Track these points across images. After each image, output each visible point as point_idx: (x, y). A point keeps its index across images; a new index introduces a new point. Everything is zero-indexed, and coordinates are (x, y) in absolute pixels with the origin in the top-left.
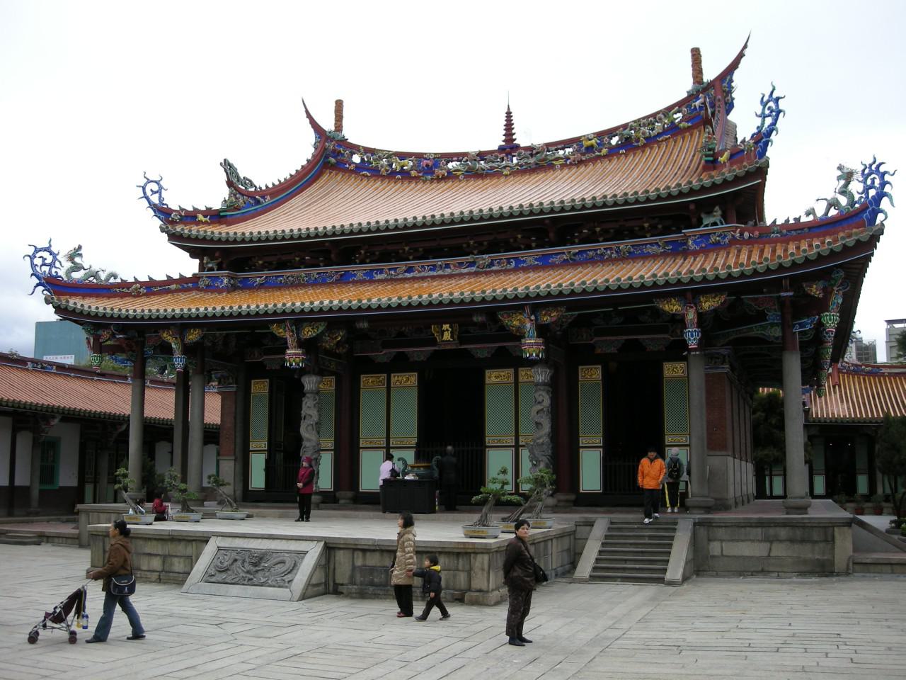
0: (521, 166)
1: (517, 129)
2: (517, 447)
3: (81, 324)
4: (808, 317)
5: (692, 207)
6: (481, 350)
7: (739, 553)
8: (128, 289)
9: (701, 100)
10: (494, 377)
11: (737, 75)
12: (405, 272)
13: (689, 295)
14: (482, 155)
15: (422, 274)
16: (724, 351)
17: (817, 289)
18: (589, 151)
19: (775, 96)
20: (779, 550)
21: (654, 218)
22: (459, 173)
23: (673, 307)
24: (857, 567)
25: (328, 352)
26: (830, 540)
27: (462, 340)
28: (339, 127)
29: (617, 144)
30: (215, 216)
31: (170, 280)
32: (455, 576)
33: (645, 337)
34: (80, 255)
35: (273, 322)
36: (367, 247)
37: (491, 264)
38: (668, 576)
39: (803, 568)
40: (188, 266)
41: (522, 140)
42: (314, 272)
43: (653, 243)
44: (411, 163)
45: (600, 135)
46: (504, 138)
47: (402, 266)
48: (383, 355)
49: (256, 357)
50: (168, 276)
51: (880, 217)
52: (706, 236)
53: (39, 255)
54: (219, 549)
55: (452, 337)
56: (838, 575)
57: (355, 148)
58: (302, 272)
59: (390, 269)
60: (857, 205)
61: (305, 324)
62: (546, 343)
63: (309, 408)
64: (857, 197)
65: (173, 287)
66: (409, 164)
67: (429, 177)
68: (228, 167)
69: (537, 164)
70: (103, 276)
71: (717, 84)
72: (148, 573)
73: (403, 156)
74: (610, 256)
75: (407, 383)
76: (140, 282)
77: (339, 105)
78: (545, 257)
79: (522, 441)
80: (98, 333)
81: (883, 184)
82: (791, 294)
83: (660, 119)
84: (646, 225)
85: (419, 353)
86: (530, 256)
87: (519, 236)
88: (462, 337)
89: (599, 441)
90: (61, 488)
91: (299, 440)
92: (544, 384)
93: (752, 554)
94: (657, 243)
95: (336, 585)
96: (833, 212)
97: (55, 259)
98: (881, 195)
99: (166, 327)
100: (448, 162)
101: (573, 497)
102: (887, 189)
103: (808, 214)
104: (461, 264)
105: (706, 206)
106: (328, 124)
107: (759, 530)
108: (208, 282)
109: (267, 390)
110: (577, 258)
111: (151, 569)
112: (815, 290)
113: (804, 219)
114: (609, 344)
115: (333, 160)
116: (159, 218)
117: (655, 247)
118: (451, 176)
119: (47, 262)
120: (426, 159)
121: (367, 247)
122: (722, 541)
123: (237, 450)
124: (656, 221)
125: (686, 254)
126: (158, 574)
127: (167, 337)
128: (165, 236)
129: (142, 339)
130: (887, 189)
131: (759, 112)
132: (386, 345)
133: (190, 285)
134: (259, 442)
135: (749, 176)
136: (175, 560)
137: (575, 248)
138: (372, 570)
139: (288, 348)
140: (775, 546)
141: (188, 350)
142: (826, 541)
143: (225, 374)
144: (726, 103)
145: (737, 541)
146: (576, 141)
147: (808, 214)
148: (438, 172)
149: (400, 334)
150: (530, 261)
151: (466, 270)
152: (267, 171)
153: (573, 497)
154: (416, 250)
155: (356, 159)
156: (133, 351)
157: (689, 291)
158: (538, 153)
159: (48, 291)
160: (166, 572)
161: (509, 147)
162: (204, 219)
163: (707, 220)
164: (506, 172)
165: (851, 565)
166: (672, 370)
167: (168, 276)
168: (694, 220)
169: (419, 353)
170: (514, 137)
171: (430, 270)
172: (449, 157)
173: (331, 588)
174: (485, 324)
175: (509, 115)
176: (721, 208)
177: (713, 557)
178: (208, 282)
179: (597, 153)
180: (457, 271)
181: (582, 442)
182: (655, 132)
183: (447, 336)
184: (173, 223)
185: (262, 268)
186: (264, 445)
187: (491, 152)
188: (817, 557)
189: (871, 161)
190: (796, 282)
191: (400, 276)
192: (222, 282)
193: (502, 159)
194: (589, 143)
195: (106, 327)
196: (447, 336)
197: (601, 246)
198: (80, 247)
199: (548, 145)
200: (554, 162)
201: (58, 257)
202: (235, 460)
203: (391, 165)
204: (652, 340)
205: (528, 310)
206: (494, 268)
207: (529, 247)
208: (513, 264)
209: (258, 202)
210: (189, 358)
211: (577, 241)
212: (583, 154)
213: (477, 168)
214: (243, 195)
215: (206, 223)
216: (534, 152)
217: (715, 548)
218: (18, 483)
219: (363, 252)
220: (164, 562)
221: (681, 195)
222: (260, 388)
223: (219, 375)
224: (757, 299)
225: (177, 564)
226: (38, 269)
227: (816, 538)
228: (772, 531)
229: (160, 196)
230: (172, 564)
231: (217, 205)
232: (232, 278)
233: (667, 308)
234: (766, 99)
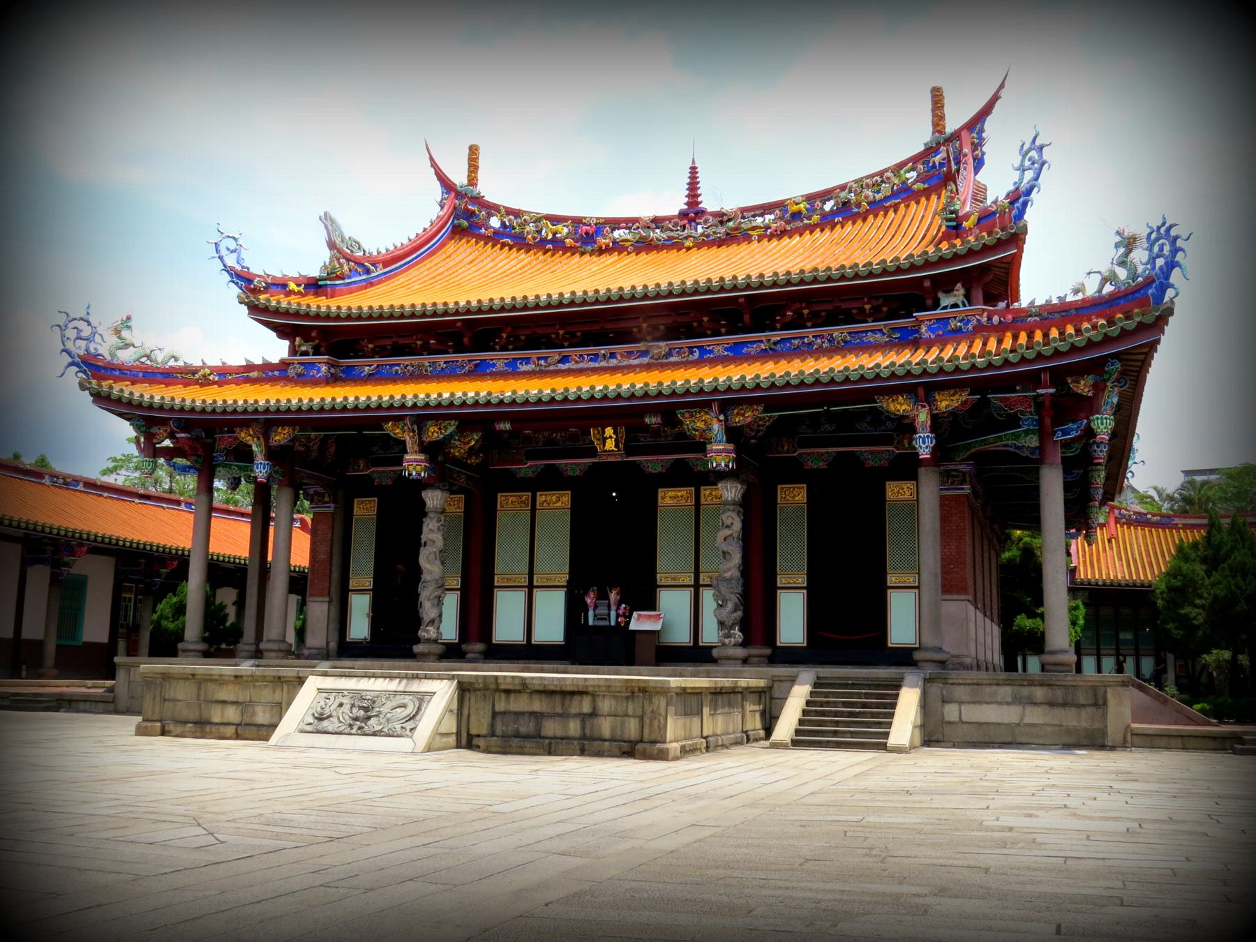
0: (708, 236)
1: (702, 190)
2: (697, 587)
3: (128, 420)
4: (1074, 421)
5: (927, 284)
6: (654, 463)
7: (983, 720)
8: (194, 373)
9: (943, 155)
10: (669, 498)
11: (990, 124)
12: (559, 362)
13: (921, 391)
14: (657, 222)
15: (581, 365)
16: (964, 468)
17: (1085, 386)
18: (792, 219)
19: (1038, 143)
20: (1034, 716)
21: (877, 298)
22: (627, 244)
23: (900, 406)
24: (1136, 739)
25: (455, 461)
26: (1099, 703)
27: (629, 450)
28: (472, 181)
29: (831, 210)
30: (314, 286)
31: (250, 367)
32: (623, 723)
33: (863, 449)
34: (129, 327)
35: (387, 419)
36: (509, 329)
37: (669, 354)
38: (892, 740)
39: (1066, 740)
40: (276, 349)
41: (709, 203)
42: (441, 359)
43: (876, 330)
44: (566, 230)
45: (810, 198)
46: (686, 200)
47: (555, 354)
48: (528, 468)
49: (362, 469)
50: (247, 361)
51: (1170, 293)
52: (944, 321)
53: (72, 325)
54: (320, 690)
55: (617, 446)
56: (1113, 748)
57: (492, 209)
58: (425, 360)
59: (539, 359)
60: (1140, 279)
61: (430, 423)
62: (737, 451)
63: (432, 533)
64: (1140, 269)
65: (254, 374)
66: (564, 230)
67: (589, 248)
68: (327, 220)
69: (728, 234)
70: (160, 357)
71: (964, 134)
73: (556, 220)
74: (821, 346)
75: (557, 504)
76: (209, 367)
77: (473, 152)
78: (736, 347)
79: (704, 579)
81: (1175, 251)
82: (1052, 391)
83: (888, 178)
84: (867, 307)
85: (573, 466)
86: (719, 344)
87: (705, 319)
88: (630, 446)
89: (802, 580)
90: (86, 644)
91: (418, 571)
92: (734, 503)
93: (999, 720)
94: (881, 330)
95: (470, 737)
96: (1108, 288)
97: (93, 334)
98: (1171, 265)
99: (245, 424)
100: (613, 230)
101: (768, 651)
102: (1179, 257)
103: (1076, 292)
104: (630, 354)
105: (945, 283)
106: (459, 177)
107: (1008, 689)
108: (300, 369)
109: (373, 512)
110: (778, 347)
112: (1083, 387)
113: (1070, 298)
114: (818, 457)
115: (465, 223)
116: (237, 284)
117: (878, 335)
118: (617, 247)
119: (84, 334)
120: (585, 224)
121: (509, 329)
122: (961, 703)
123: (333, 590)
124: (880, 301)
125: (916, 344)
127: (245, 436)
128: (244, 309)
129: (209, 441)
130: (1179, 257)
131: (1017, 165)
132: (533, 455)
133: (276, 373)
134: (363, 576)
135: (1000, 244)
137: (776, 336)
138: (518, 714)
140: (1029, 709)
141: (273, 454)
142: (1096, 705)
143: (320, 489)
144: (974, 159)
145: (980, 703)
146: (780, 205)
147: (1076, 292)
148: (602, 241)
149: (550, 442)
150: (719, 351)
152: (379, 234)
153: (768, 651)
154: (573, 335)
155: (495, 222)
156: (199, 456)
157: (922, 387)
158: (729, 220)
159: (84, 372)
160: (246, 725)
161: (693, 212)
162: (296, 289)
163: (946, 300)
164: (688, 243)
165: (1129, 736)
166: (897, 491)
167: (247, 361)
168: (929, 302)
169: (573, 466)
170: (700, 199)
171: (591, 360)
172: (615, 223)
173: (464, 741)
174: (657, 426)
175: (693, 171)
176: (963, 286)
177: (949, 723)
178: (300, 369)
179: (806, 221)
180: (625, 363)
181: (781, 581)
184: (256, 291)
185: (373, 354)
186: (368, 583)
187: (669, 219)
188: (1084, 724)
189: (1159, 224)
190: (1058, 376)
191: (552, 368)
192: (319, 371)
193: (684, 227)
194: (795, 208)
195: (163, 422)
196: (610, 445)
197: (809, 333)
198: (129, 318)
199: (743, 210)
200: (751, 233)
201: (100, 330)
202: (329, 602)
203: (539, 232)
204: (872, 453)
205: (715, 407)
206: (672, 359)
208: (697, 355)
209: (368, 271)
210: (273, 466)
211: (778, 326)
212: (788, 222)
213: (648, 238)
214: (348, 260)
215: (299, 293)
216: (725, 218)
217: (951, 712)
218: (27, 634)
219: (504, 335)
220: (242, 714)
221: (913, 268)
222: (365, 510)
223: (311, 491)
224: (1009, 398)
226: (70, 345)
227: (1082, 700)
228: (1025, 691)
229: (239, 256)
230: (254, 714)
231: (314, 272)
232: (333, 366)
233: (892, 407)
234: (1026, 148)
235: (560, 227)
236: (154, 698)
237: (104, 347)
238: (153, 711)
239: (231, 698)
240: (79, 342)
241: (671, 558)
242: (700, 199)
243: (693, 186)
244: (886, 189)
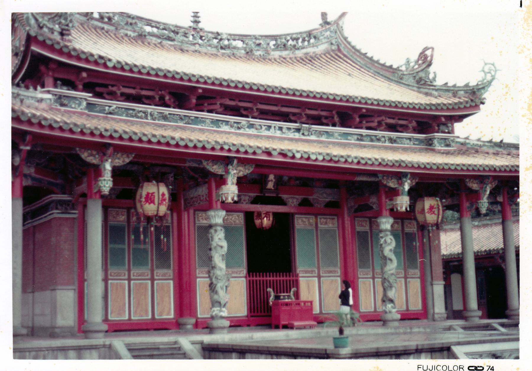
94: (410, 139)
137: (364, 132)
172: (149, 22)
207: (334, 125)
211: (364, 126)
242: (200, 19)
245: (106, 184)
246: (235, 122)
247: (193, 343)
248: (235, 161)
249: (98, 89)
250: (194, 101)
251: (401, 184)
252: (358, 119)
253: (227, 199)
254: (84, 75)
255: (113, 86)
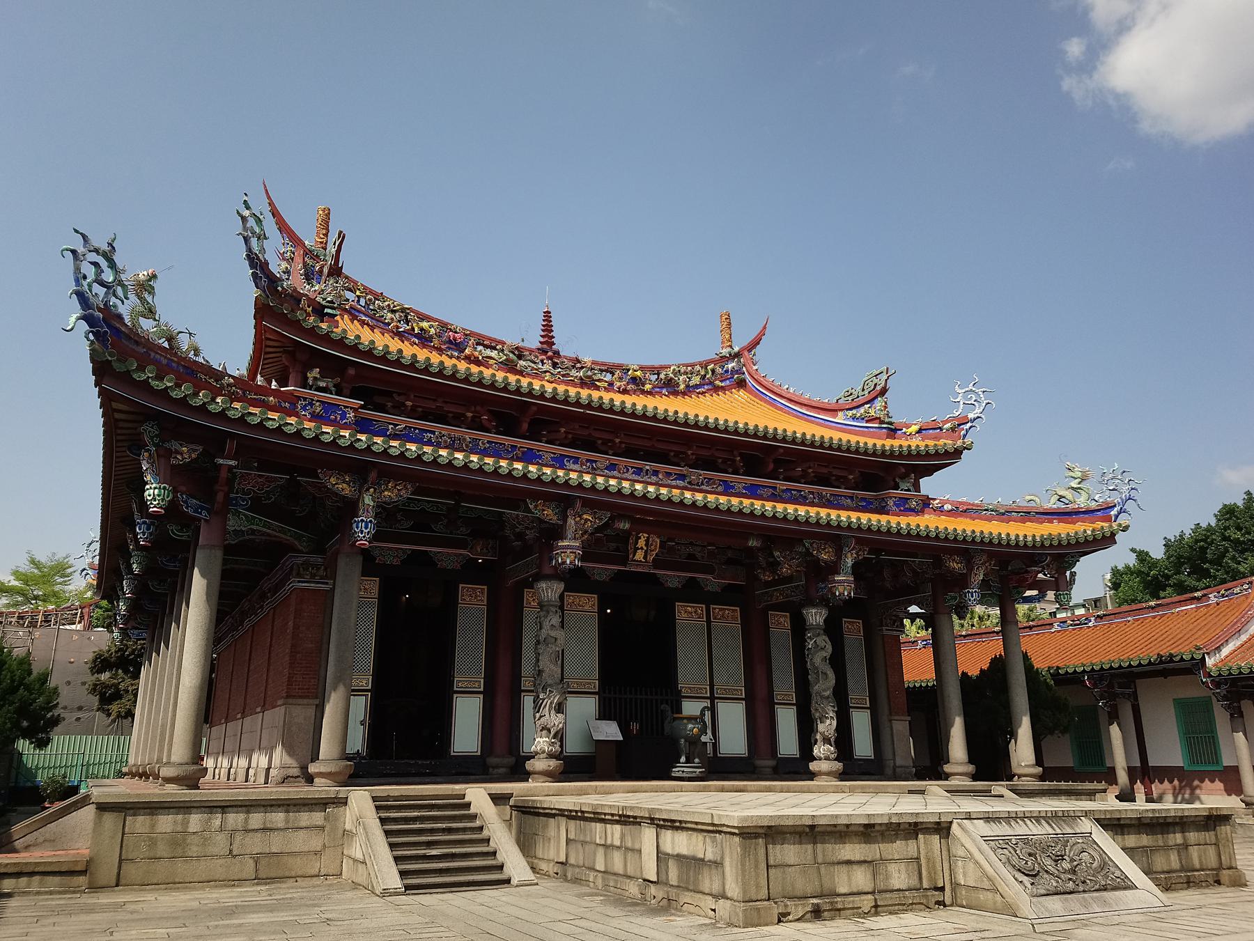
6: (673, 579)
10: (687, 615)
22: (491, 362)
27: (657, 563)
34: (151, 291)
35: (536, 496)
41: (566, 345)
42: (484, 437)
44: (432, 331)
45: (642, 368)
55: (645, 557)
58: (468, 434)
59: (588, 461)
70: (184, 343)
72: (857, 898)
80: (167, 445)
104: (668, 474)
108: (318, 409)
111: (855, 890)
126: (870, 897)
136: (892, 868)
137: (782, 485)
139: (562, 538)
151: (674, 483)
153: (772, 763)
160: (880, 892)
169: (602, 571)
175: (547, 315)
178: (318, 409)
182: (691, 383)
183: (639, 556)
187: (531, 351)
192: (344, 416)
197: (806, 488)
199: (594, 363)
206: (704, 487)
219: (563, 430)
225: (896, 875)
235: (425, 325)
236: (756, 867)
237: (126, 309)
238: (758, 886)
239: (858, 857)
240: (97, 289)
241: (689, 668)
243: (548, 328)
244: (696, 380)
245: (363, 530)
246: (588, 461)
247: (497, 799)
248: (578, 504)
249: (378, 399)
250: (525, 426)
251: (839, 553)
252: (771, 466)
253: (564, 563)
254: (352, 371)
255: (399, 394)
